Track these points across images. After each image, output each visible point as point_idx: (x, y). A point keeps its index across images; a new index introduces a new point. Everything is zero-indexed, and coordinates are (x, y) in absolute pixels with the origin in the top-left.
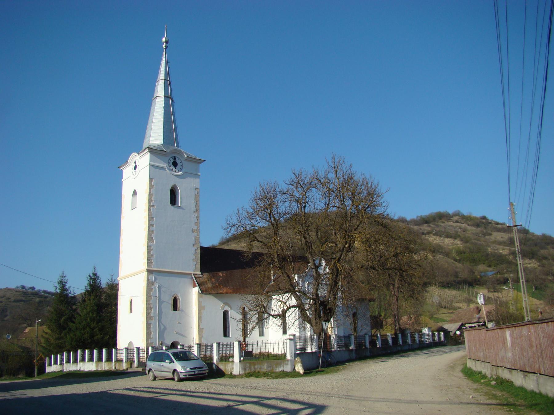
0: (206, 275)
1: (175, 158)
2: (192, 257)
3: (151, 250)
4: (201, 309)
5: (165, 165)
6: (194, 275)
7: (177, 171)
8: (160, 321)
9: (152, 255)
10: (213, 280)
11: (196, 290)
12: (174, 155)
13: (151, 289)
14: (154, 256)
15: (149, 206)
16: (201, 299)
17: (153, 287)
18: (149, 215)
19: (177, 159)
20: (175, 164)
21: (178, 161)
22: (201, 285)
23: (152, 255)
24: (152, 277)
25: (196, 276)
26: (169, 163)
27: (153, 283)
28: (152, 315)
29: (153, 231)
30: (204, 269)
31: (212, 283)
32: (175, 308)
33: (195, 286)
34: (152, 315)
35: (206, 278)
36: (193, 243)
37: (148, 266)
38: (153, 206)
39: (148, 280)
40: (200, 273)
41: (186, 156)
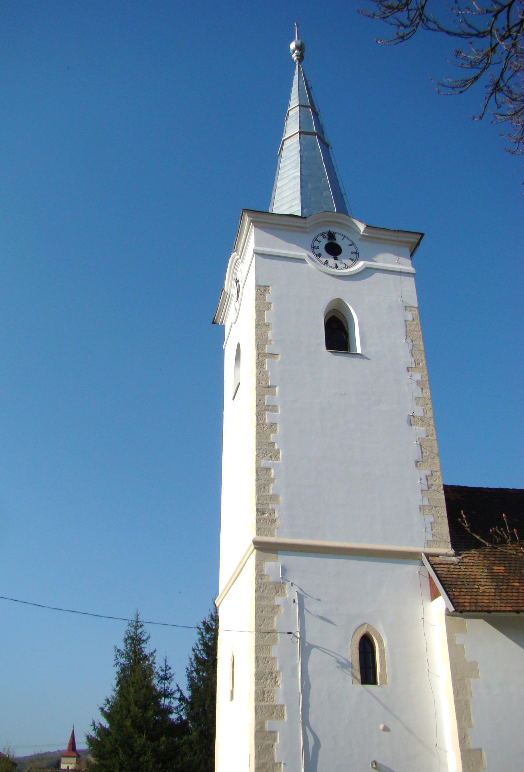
0: (472, 557)
1: (331, 236)
2: (417, 499)
3: (270, 481)
4: (462, 674)
5: (303, 253)
6: (428, 555)
7: (340, 265)
8: (306, 723)
9: (274, 498)
10: (499, 569)
11: (441, 604)
12: (326, 229)
13: (275, 609)
14: (281, 499)
15: (258, 356)
16: (459, 639)
17: (278, 600)
18: (258, 381)
19: (337, 237)
20: (334, 250)
21: (339, 241)
22: (450, 584)
23: (274, 498)
24: (274, 565)
25: (437, 560)
26: (319, 255)
27: (279, 588)
28: (279, 699)
29: (273, 425)
30: (460, 540)
31: (493, 577)
32: (368, 673)
33: (435, 595)
34: (279, 699)
35: (473, 564)
36: (417, 456)
37: (259, 530)
38: (272, 355)
39: (260, 575)
40: (452, 552)
41: (361, 227)
